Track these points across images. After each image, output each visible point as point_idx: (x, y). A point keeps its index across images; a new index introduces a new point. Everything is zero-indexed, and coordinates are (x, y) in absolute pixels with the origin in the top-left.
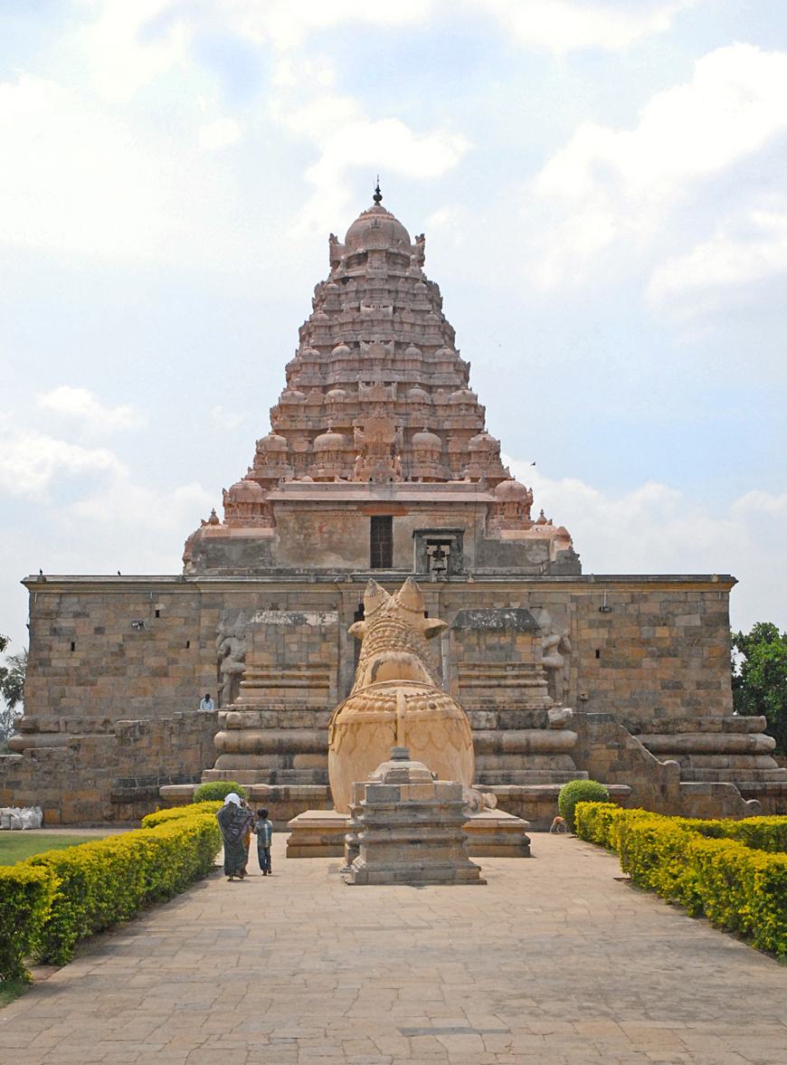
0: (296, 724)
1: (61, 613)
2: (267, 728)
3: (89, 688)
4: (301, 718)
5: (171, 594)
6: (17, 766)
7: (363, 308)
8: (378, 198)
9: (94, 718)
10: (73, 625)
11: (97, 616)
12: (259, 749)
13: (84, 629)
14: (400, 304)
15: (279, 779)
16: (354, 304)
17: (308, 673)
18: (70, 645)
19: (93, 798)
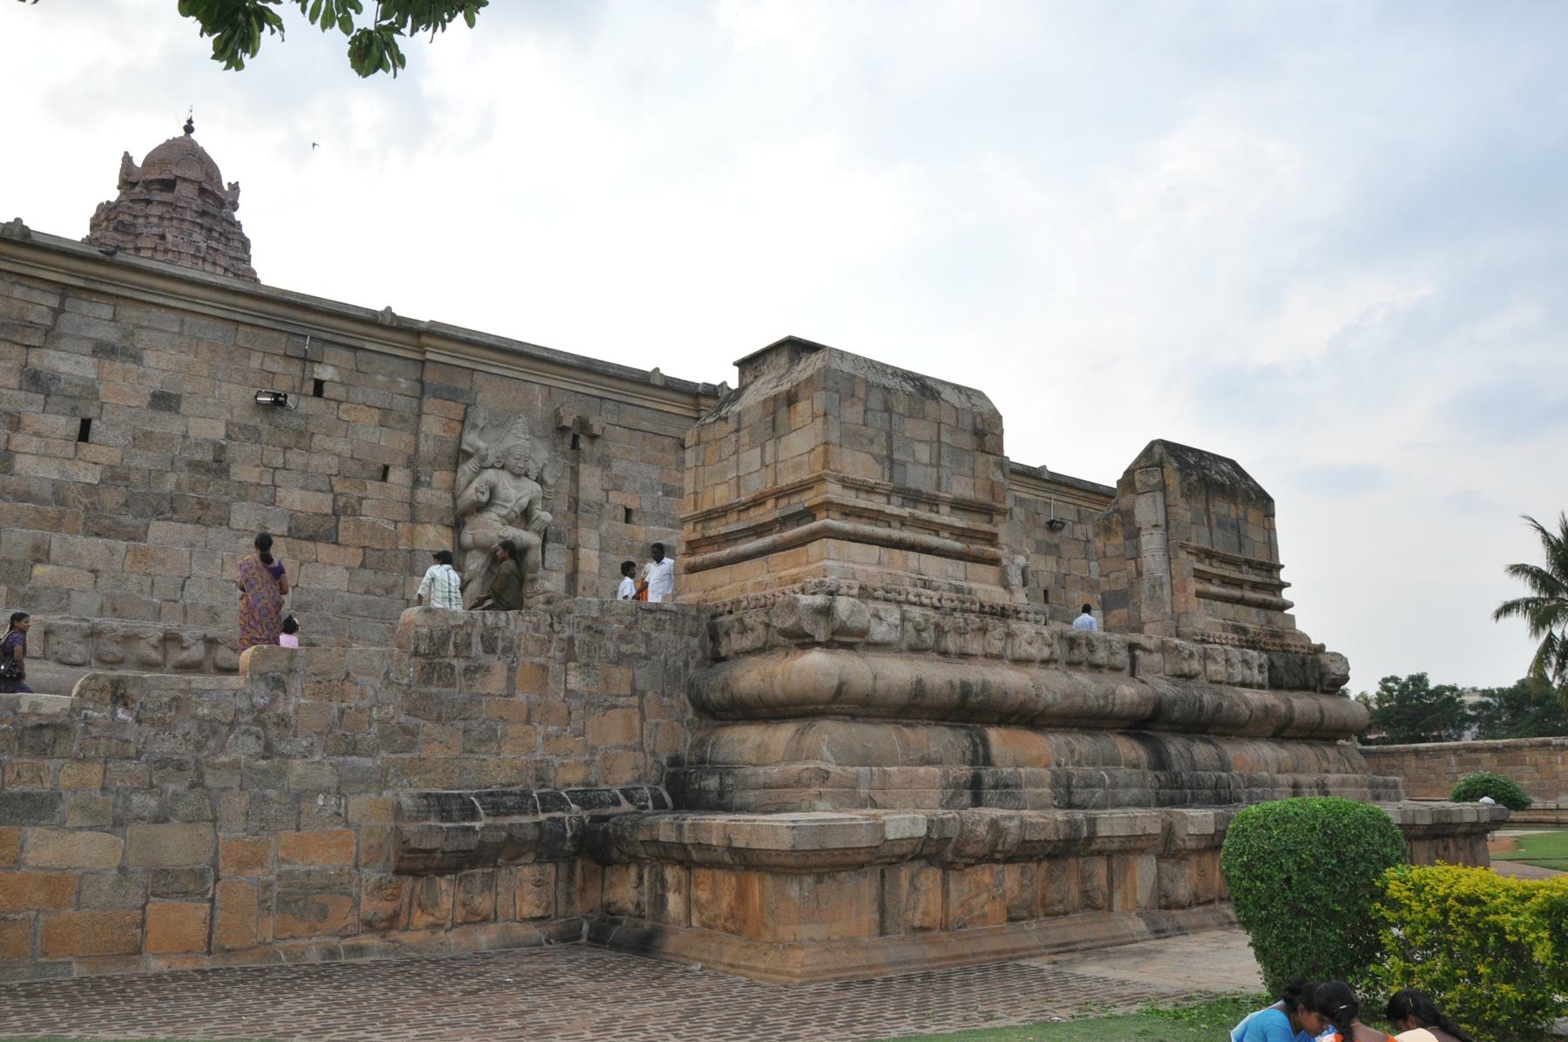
0: (975, 646)
1: (60, 336)
2: (916, 649)
3: (122, 545)
4: (983, 630)
5: (355, 349)
6: (48, 736)
7: (169, 237)
8: (189, 129)
9: (134, 625)
10: (91, 374)
11: (162, 362)
12: (913, 708)
13: (122, 390)
14: (214, 244)
15: (988, 794)
16: (155, 230)
17: (959, 521)
18: (78, 423)
19: (324, 858)
